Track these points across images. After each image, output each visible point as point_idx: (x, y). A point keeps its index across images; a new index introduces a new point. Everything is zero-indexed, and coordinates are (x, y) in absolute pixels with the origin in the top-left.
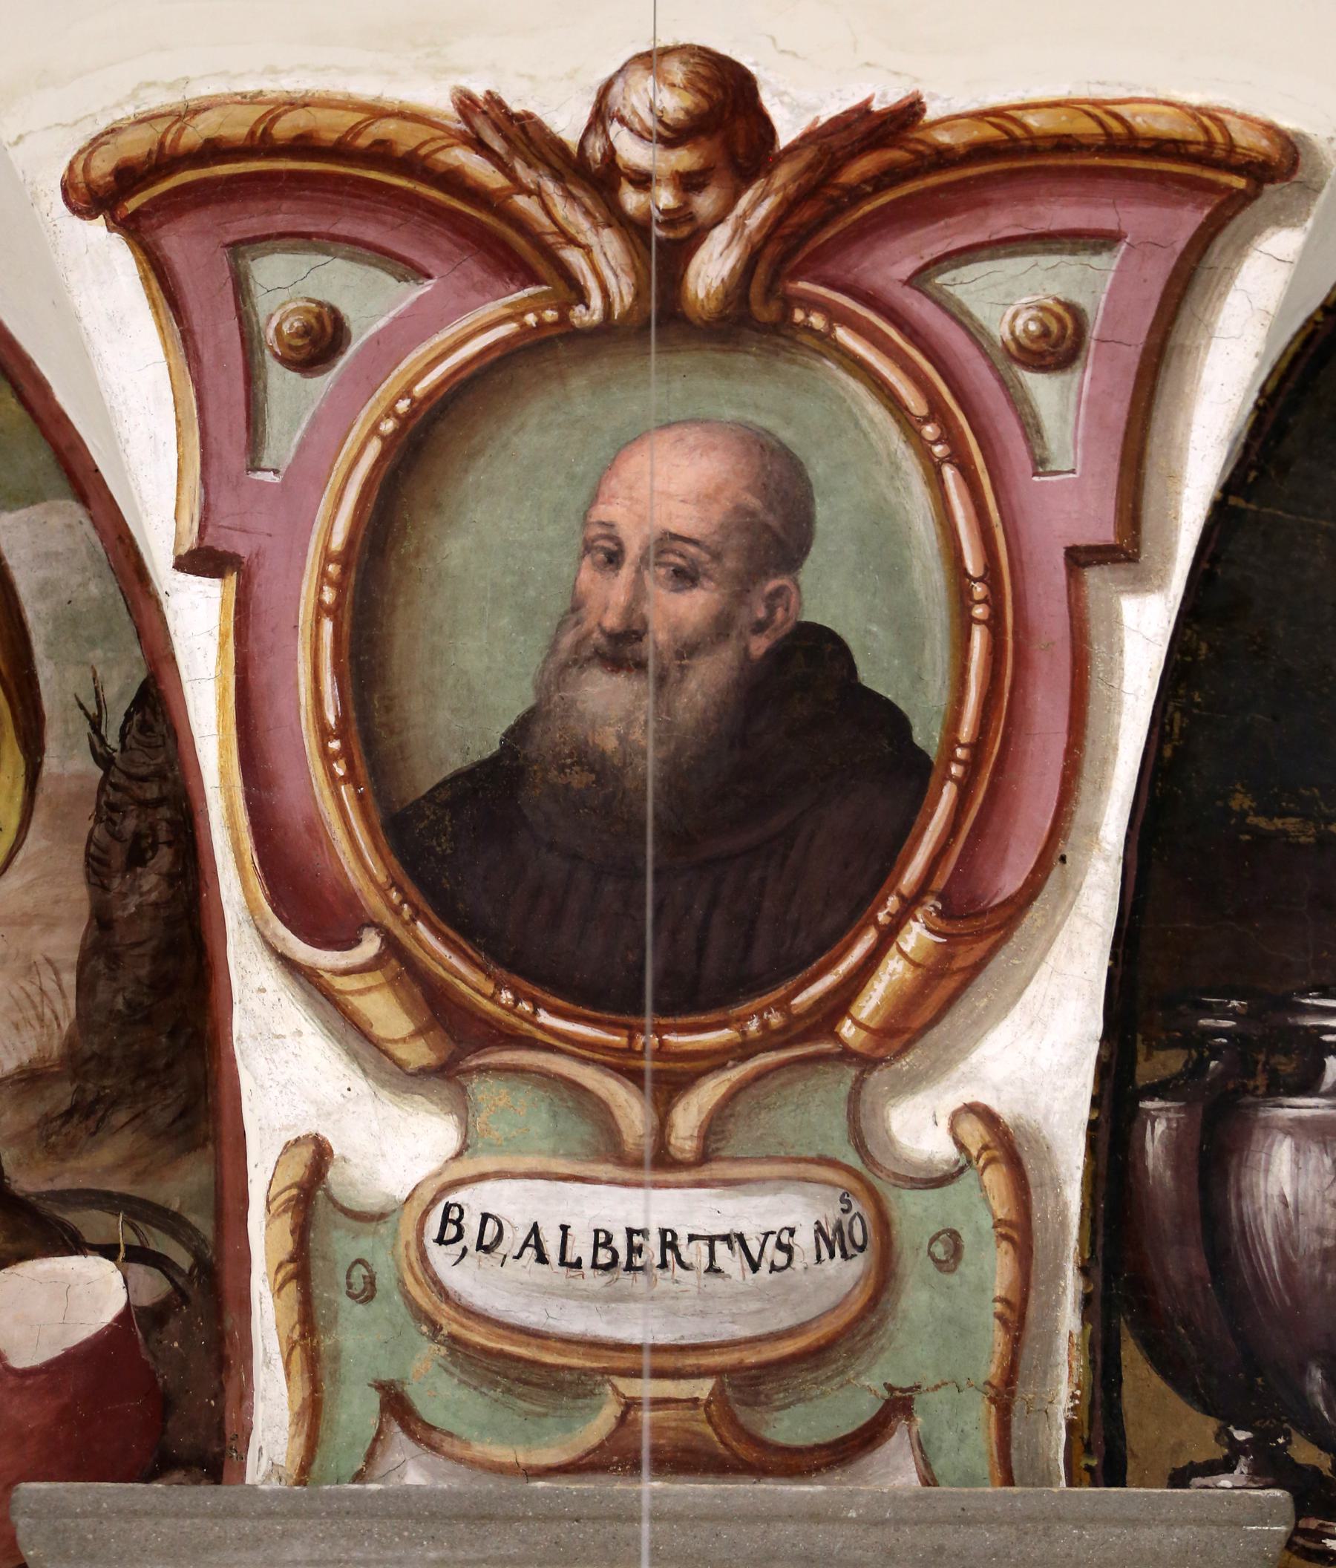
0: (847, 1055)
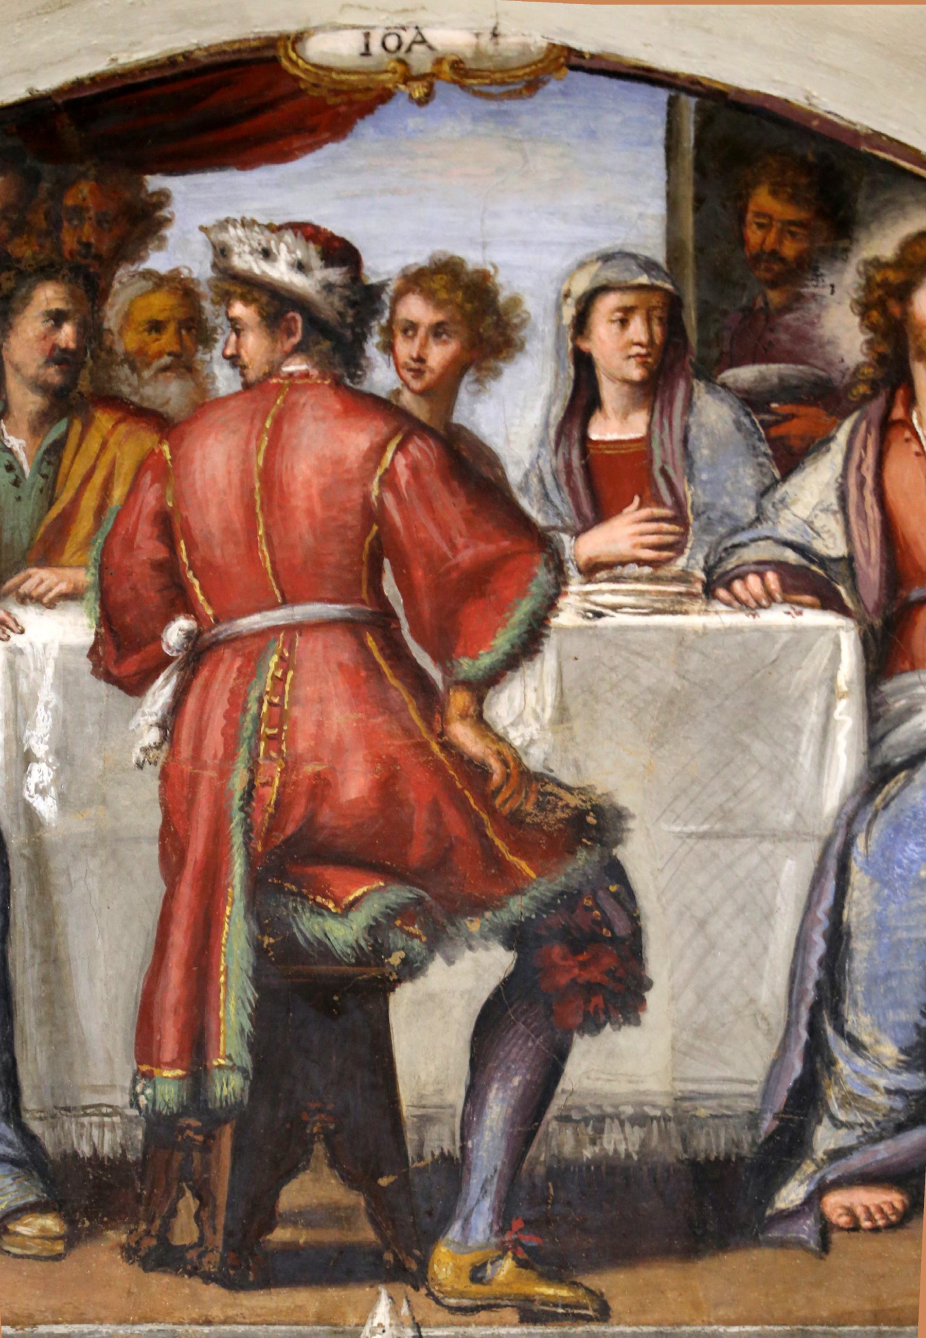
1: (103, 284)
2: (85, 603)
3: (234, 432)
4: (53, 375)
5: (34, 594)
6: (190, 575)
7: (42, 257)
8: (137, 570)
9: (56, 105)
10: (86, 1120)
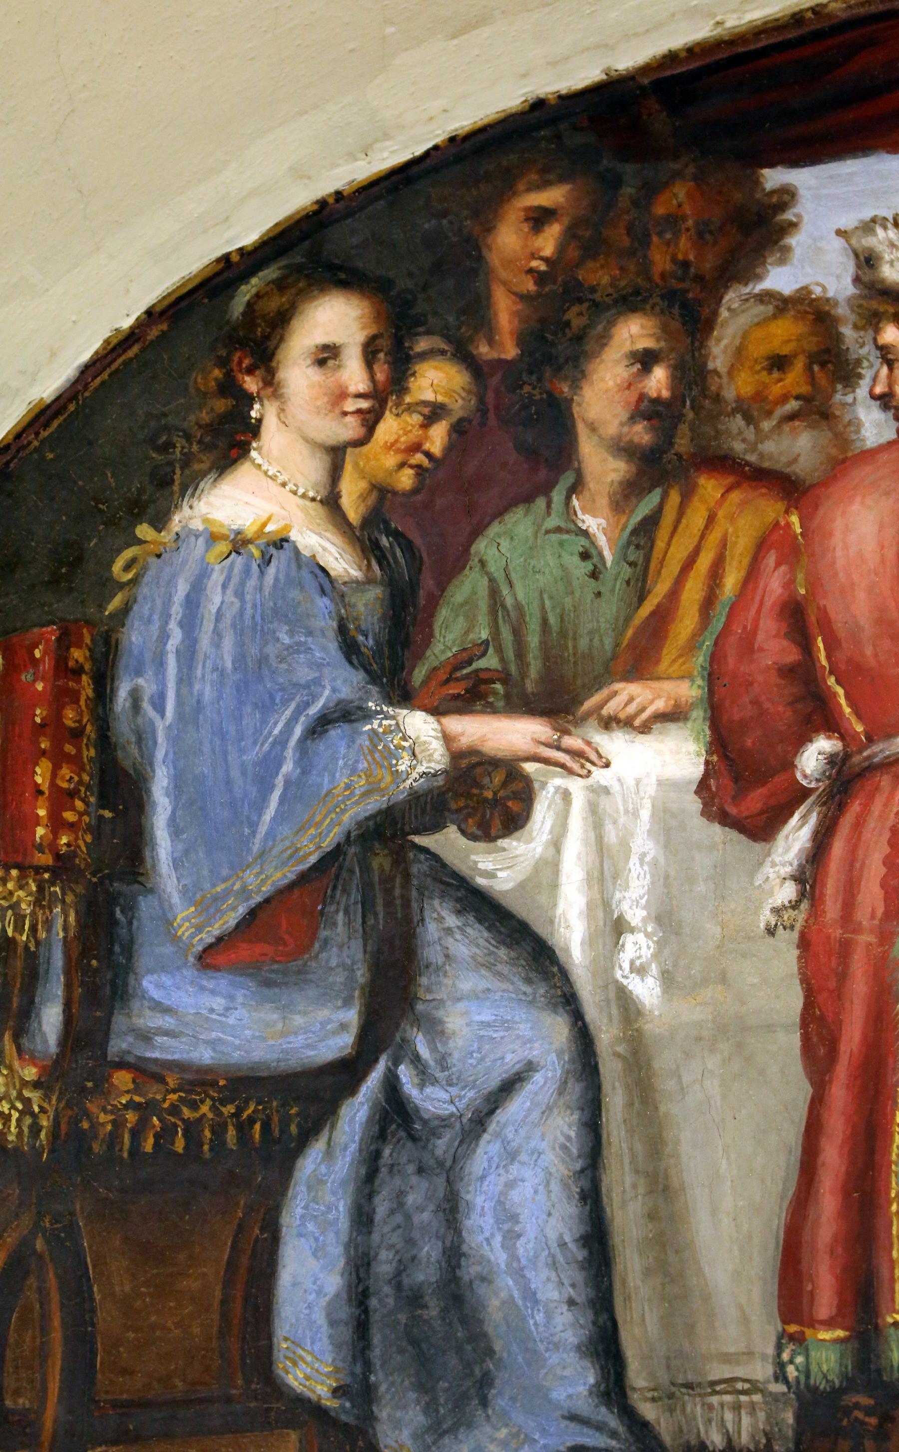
1: (706, 312)
2: (689, 724)
3: (888, 494)
4: (641, 434)
5: (622, 716)
6: (831, 681)
7: (623, 283)
8: (760, 678)
9: (642, 88)
10: (715, 1400)
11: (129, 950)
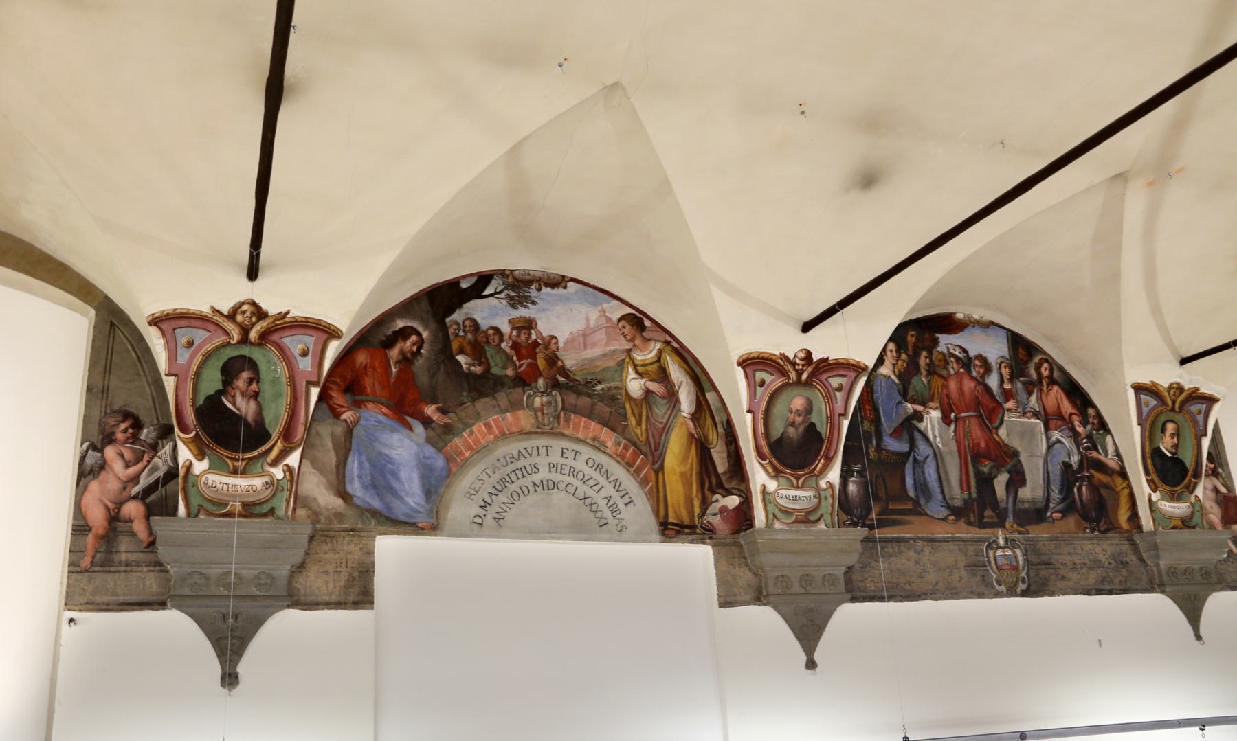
0: (816, 475)
11: (881, 433)
